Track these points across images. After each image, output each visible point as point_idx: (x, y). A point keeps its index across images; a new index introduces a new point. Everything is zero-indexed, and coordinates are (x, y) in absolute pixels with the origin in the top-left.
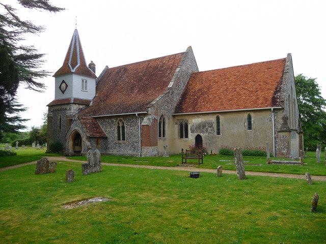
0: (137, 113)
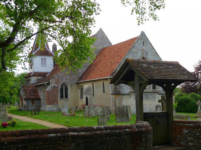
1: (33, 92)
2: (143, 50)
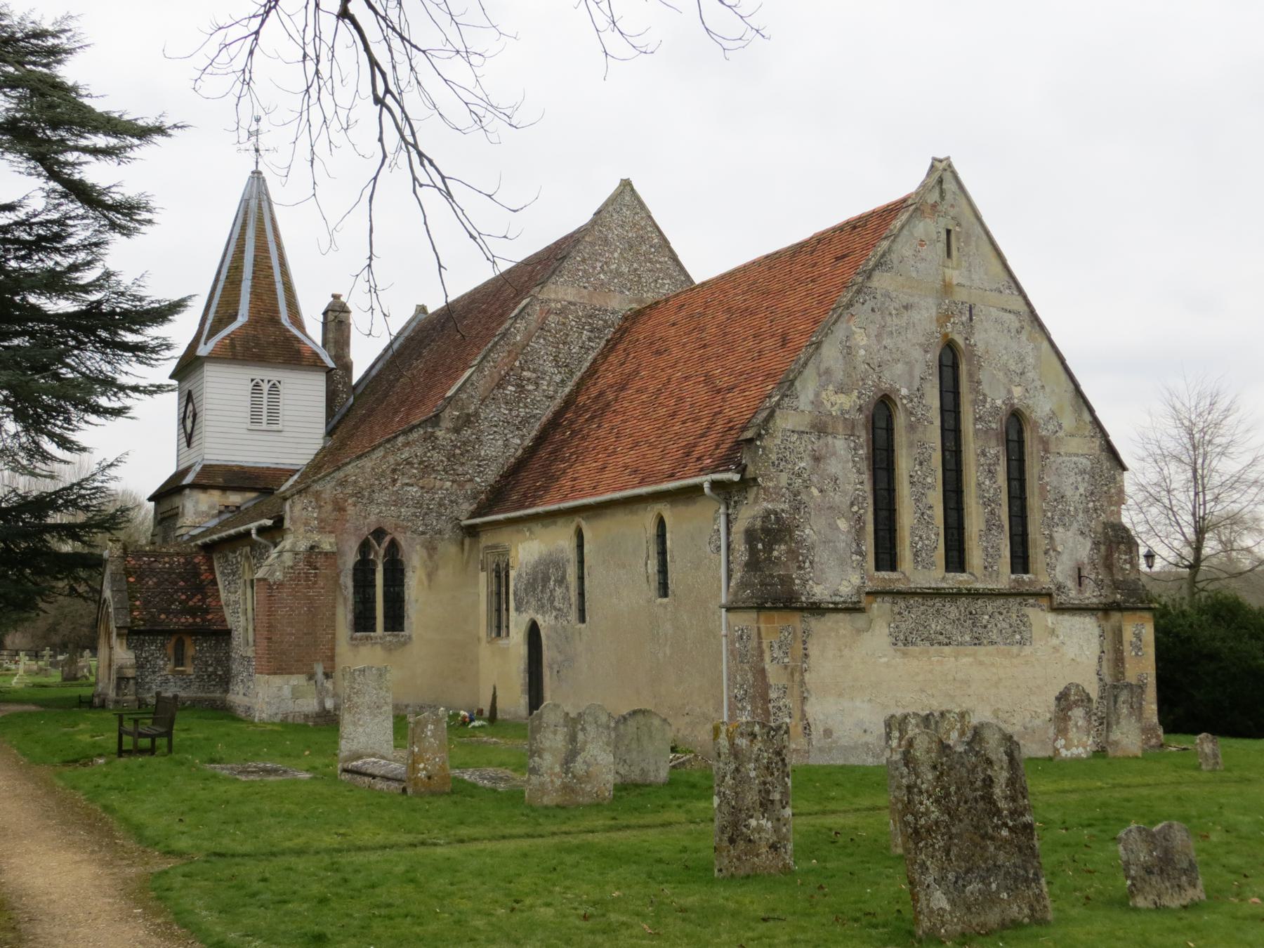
0: (253, 526)
1: (181, 589)
2: (947, 288)
